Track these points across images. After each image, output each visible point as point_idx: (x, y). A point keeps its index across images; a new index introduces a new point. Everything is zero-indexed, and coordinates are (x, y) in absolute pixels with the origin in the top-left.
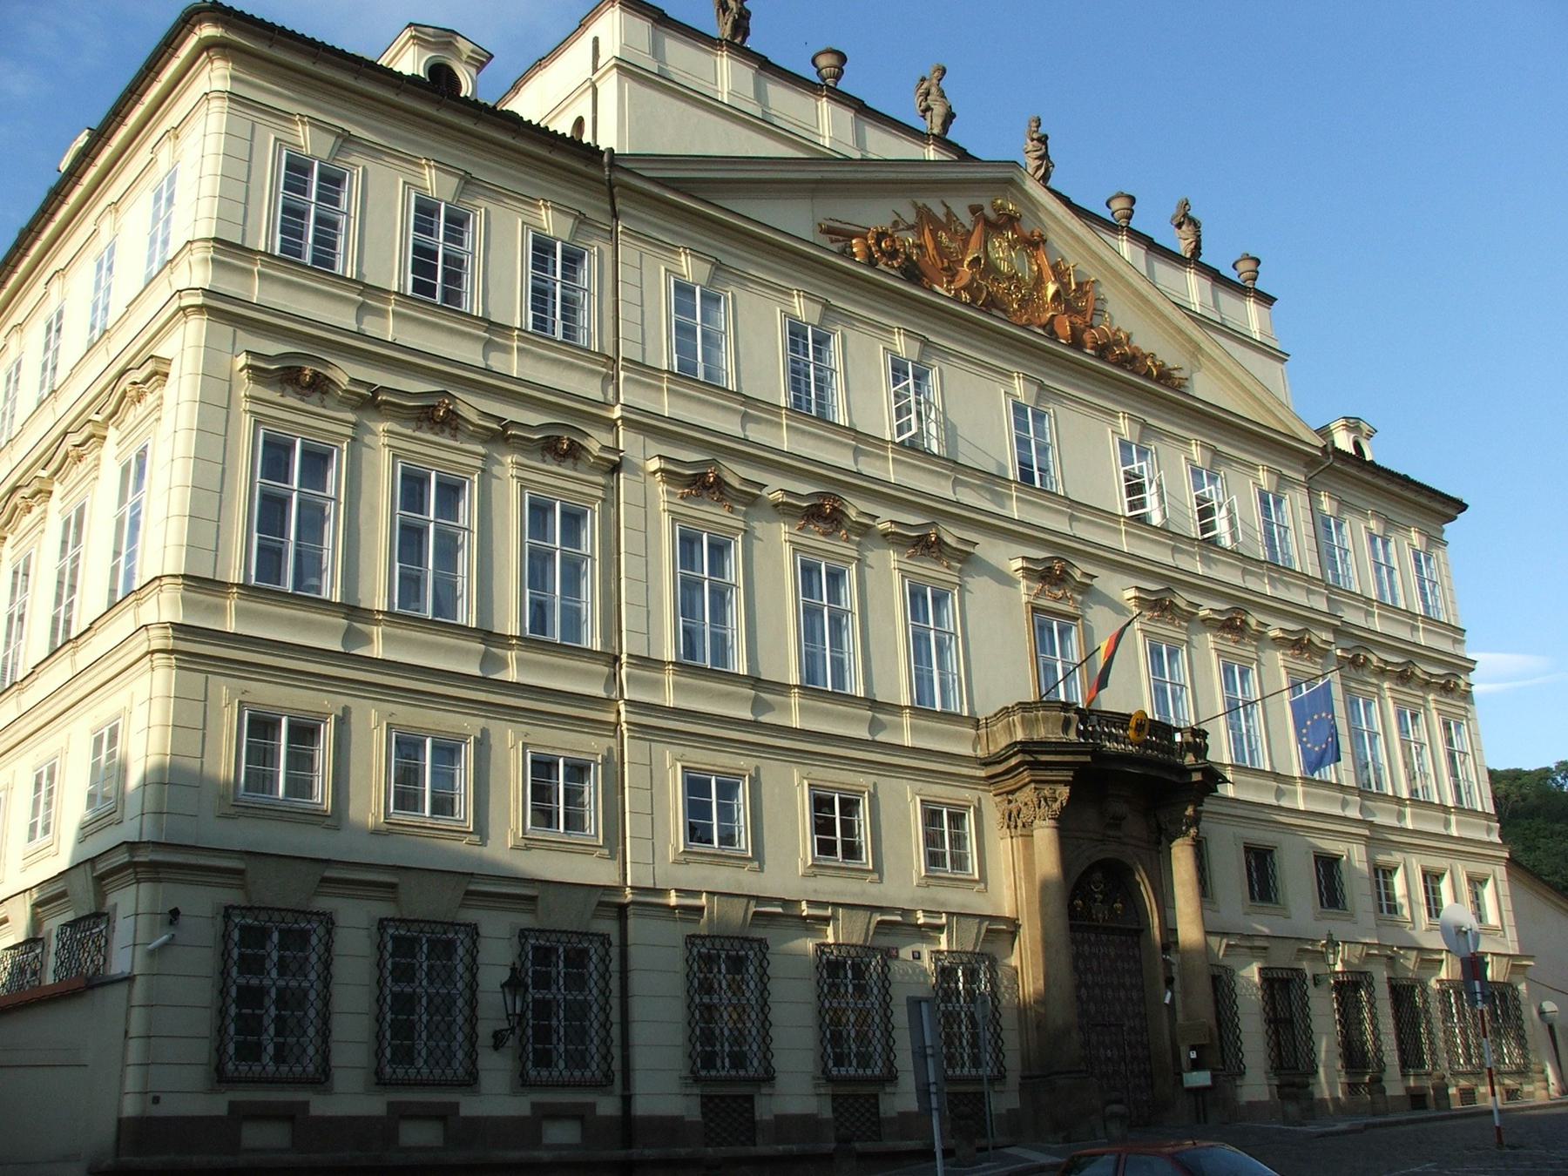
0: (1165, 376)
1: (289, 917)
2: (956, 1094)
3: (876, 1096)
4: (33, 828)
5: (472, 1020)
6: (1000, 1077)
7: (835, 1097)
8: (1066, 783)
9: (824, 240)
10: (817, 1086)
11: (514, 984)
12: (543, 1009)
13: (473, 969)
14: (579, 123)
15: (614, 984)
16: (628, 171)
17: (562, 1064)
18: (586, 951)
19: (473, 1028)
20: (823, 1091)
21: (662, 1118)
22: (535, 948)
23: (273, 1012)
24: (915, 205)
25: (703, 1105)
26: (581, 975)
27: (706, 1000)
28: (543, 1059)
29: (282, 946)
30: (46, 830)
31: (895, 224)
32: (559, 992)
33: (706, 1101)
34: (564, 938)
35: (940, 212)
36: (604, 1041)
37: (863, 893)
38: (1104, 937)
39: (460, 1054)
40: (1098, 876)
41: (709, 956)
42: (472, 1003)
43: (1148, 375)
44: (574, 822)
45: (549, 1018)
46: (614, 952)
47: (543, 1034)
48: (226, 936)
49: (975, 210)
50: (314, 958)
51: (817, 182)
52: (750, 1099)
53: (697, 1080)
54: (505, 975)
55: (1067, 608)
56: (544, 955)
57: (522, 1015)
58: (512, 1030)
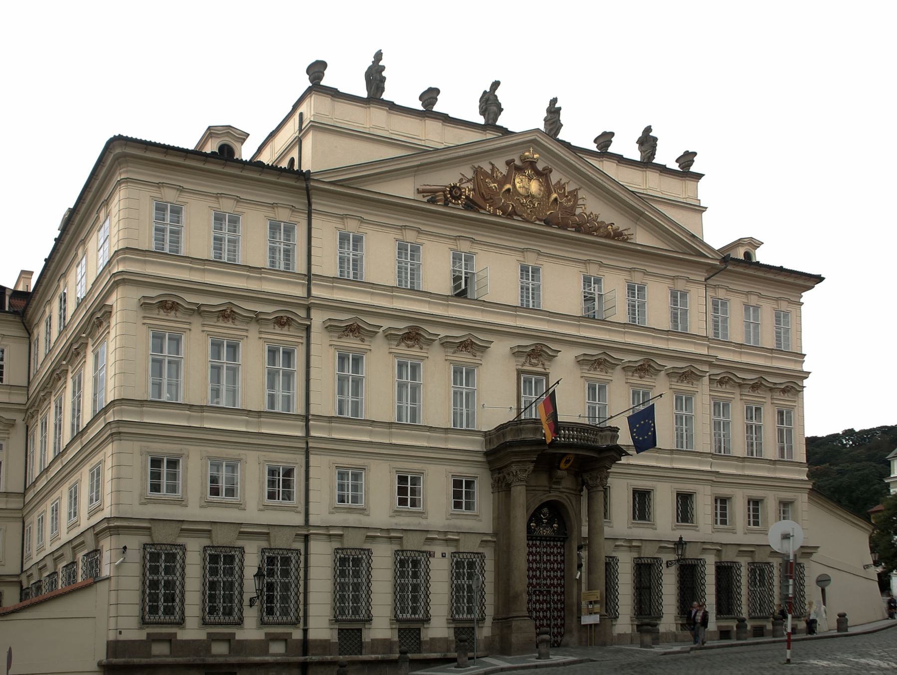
0: (618, 235)
1: (168, 548)
4: (70, 513)
5: (241, 593)
11: (259, 575)
12: (271, 587)
13: (242, 569)
14: (292, 160)
15: (302, 574)
17: (278, 614)
18: (290, 557)
19: (242, 596)
22: (268, 557)
23: (163, 591)
26: (287, 570)
27: (342, 580)
28: (270, 611)
29: (165, 561)
30: (75, 513)
32: (277, 579)
34: (281, 552)
35: (487, 168)
36: (296, 602)
39: (236, 609)
40: (545, 510)
41: (345, 558)
42: (241, 585)
43: (608, 236)
44: (288, 496)
45: (273, 591)
46: (302, 558)
47: (270, 599)
48: (144, 557)
49: (508, 163)
50: (178, 566)
54: (255, 571)
56: (271, 561)
57: (262, 590)
58: (258, 597)
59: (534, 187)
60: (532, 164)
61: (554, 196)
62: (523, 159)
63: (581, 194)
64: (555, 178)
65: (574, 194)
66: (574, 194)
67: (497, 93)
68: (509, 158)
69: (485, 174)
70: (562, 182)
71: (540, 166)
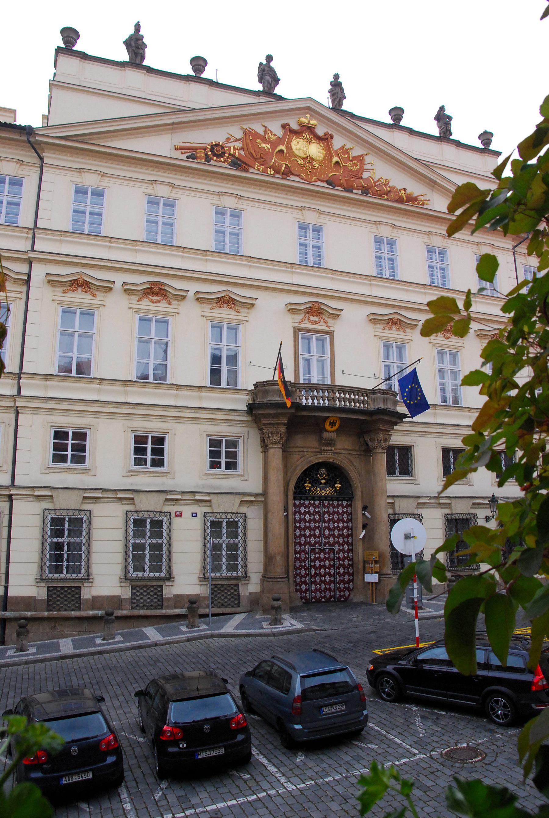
0: (411, 199)
2: (215, 586)
3: (162, 587)
6: (246, 576)
7: (133, 588)
8: (285, 424)
9: (178, 154)
10: (121, 582)
16: (43, 135)
20: (123, 584)
21: (22, 598)
24: (242, 128)
25: (49, 591)
31: (228, 139)
33: (50, 590)
35: (260, 130)
37: (163, 484)
38: (326, 503)
40: (323, 470)
49: (284, 126)
51: (173, 124)
52: (79, 588)
53: (42, 579)
55: (321, 327)
59: (315, 150)
60: (310, 129)
61: (335, 159)
62: (301, 124)
63: (368, 159)
64: (337, 143)
65: (360, 159)
66: (360, 159)
67: (272, 64)
68: (285, 122)
69: (256, 135)
70: (347, 147)
71: (320, 131)
